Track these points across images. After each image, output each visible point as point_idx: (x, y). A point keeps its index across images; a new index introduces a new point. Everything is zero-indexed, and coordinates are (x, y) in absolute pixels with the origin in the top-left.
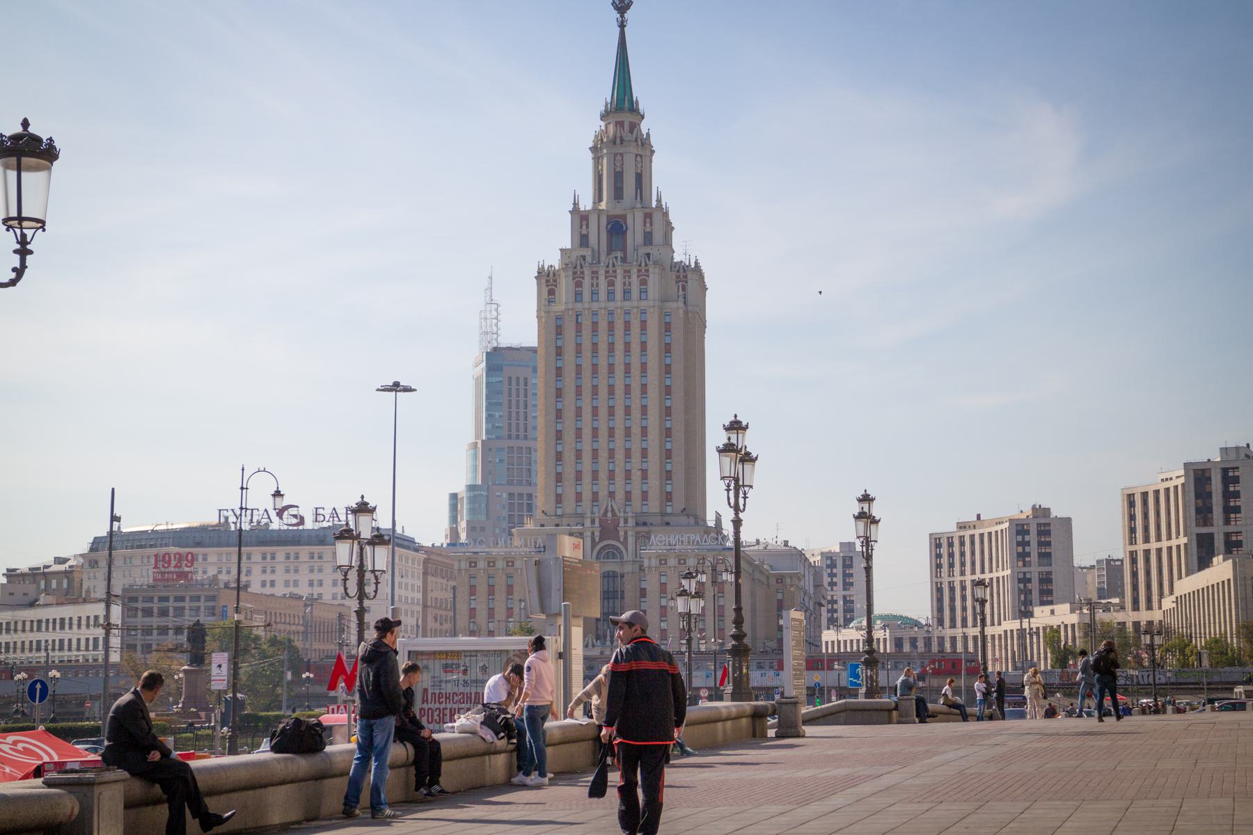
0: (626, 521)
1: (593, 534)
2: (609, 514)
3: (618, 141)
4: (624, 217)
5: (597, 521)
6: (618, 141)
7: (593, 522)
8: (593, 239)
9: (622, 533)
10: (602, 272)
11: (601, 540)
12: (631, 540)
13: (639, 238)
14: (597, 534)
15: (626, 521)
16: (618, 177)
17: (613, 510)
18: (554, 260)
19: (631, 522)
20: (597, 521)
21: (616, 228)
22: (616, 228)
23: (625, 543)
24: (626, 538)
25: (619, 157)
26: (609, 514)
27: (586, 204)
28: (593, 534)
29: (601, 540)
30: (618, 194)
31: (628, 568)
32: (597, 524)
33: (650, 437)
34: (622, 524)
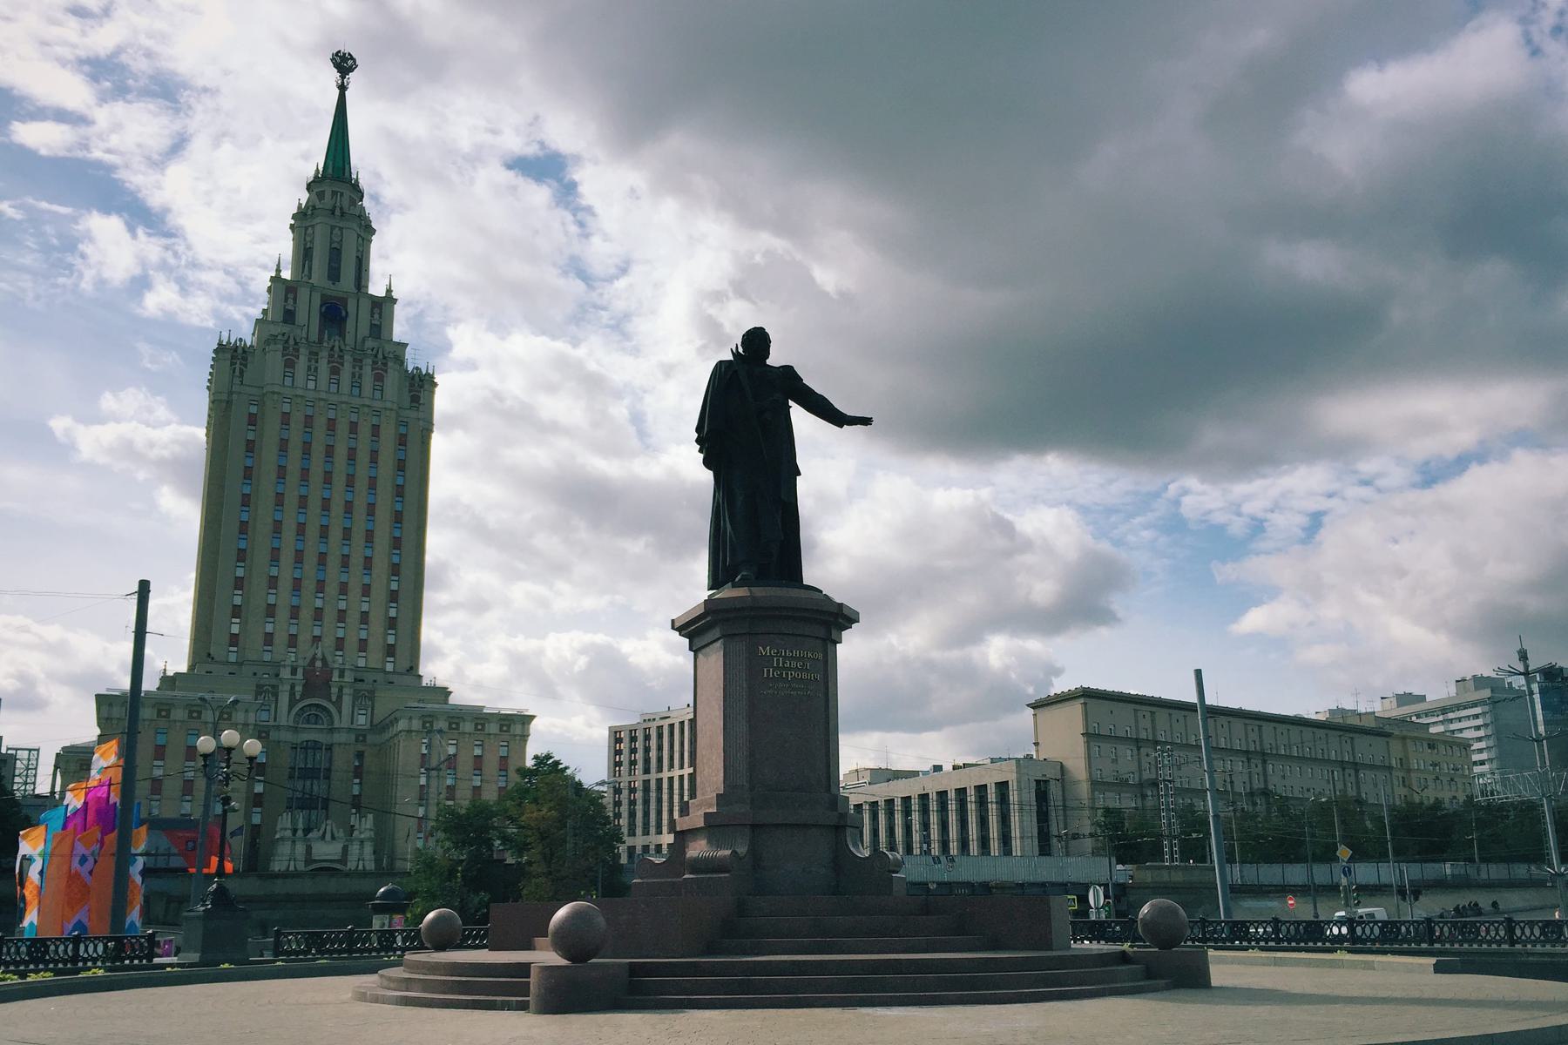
0: (342, 675)
1: (293, 687)
2: (319, 664)
3: (338, 212)
4: (344, 301)
5: (300, 671)
6: (338, 212)
7: (294, 672)
8: (301, 317)
9: (334, 690)
10: (324, 354)
11: (303, 697)
12: (347, 700)
13: (364, 329)
14: (299, 688)
15: (342, 675)
16: (335, 254)
17: (324, 660)
18: (245, 332)
19: (349, 677)
20: (300, 671)
21: (333, 314)
22: (333, 314)
23: (338, 704)
24: (340, 697)
25: (336, 231)
26: (319, 664)
27: (286, 274)
28: (293, 687)
29: (302, 698)
30: (334, 274)
31: (338, 738)
32: (300, 675)
33: (375, 571)
34: (335, 678)
